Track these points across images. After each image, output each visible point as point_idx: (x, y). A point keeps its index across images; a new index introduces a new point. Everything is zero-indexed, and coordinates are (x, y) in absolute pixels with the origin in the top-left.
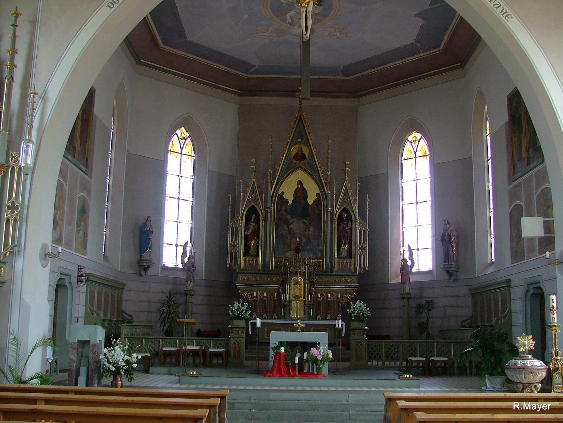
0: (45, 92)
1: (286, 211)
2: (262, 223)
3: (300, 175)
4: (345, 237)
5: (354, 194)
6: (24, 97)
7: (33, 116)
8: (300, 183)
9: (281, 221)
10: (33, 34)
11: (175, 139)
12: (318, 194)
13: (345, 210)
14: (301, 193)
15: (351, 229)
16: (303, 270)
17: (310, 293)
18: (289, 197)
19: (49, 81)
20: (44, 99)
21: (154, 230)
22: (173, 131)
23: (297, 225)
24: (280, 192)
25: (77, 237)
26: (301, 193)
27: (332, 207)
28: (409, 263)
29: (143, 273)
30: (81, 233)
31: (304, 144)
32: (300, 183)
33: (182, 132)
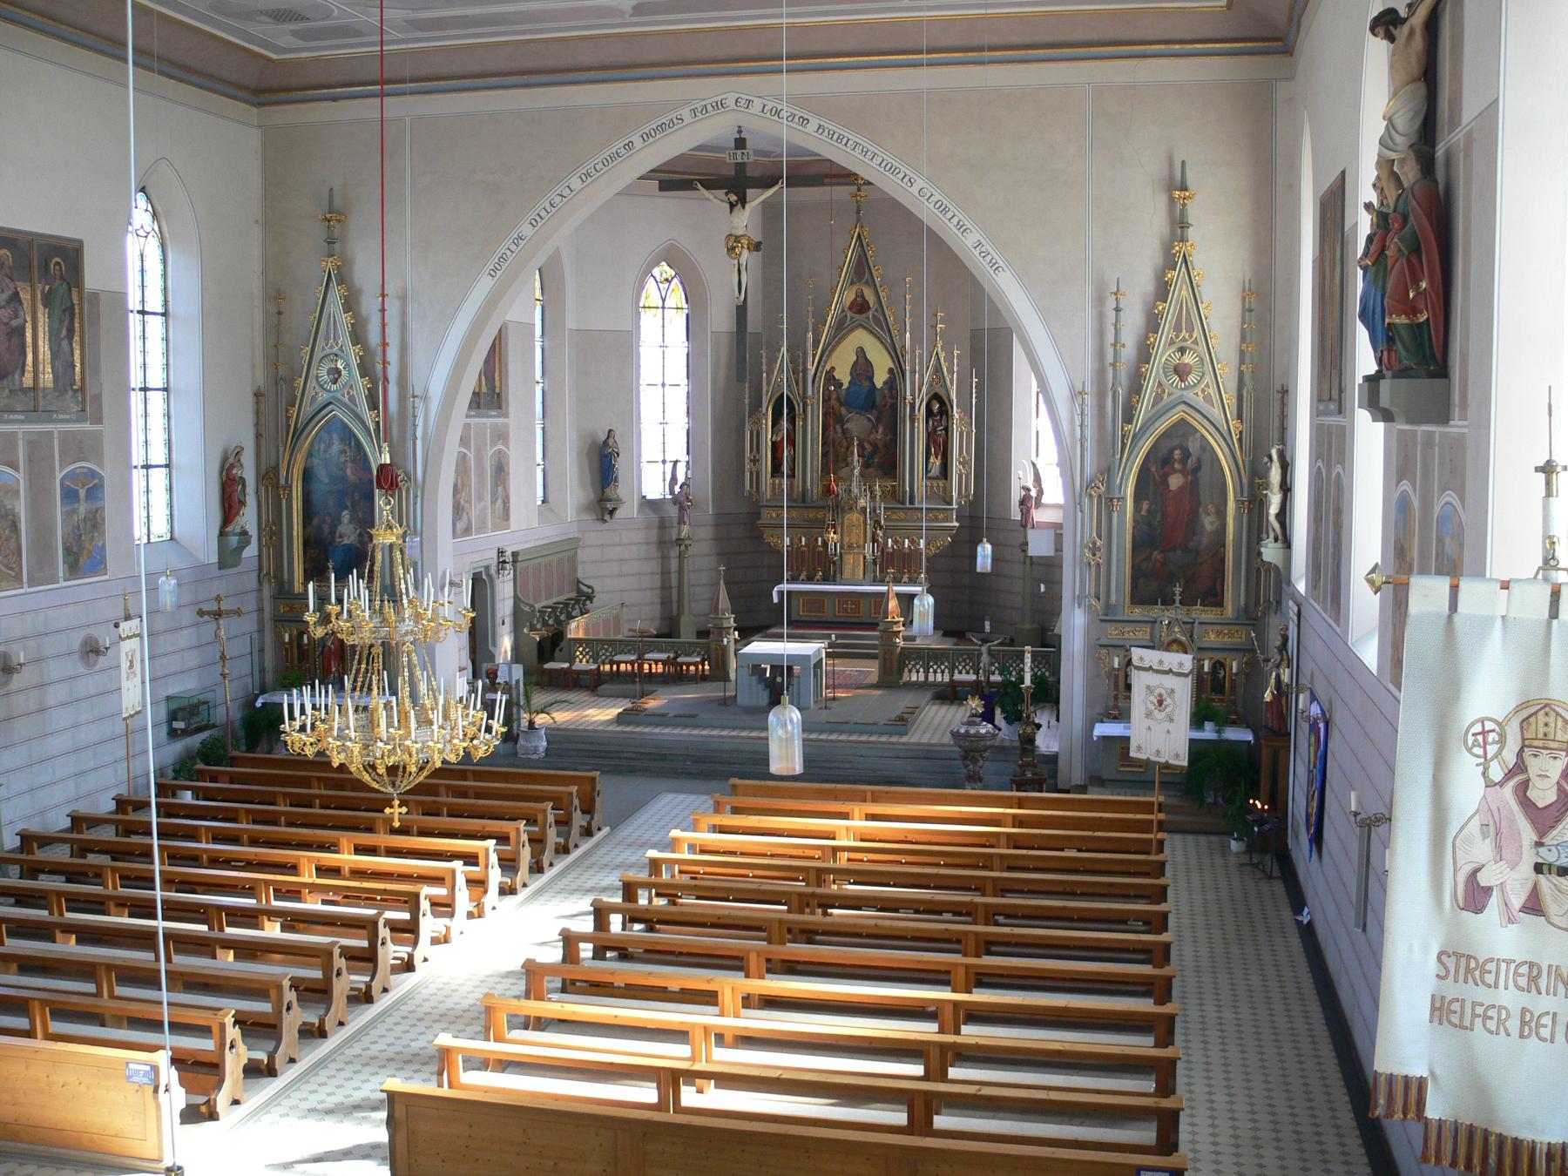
0: (426, 390)
1: (838, 399)
2: (799, 423)
3: (860, 338)
4: (939, 443)
5: (951, 372)
6: (402, 398)
7: (415, 426)
8: (861, 352)
9: (832, 418)
10: (403, 314)
11: (651, 285)
12: (891, 370)
13: (936, 397)
14: (863, 367)
15: (946, 429)
16: (862, 503)
17: (874, 540)
18: (844, 376)
19: (431, 368)
20: (426, 398)
21: (622, 448)
22: (648, 272)
23: (857, 424)
24: (828, 367)
25: (493, 511)
26: (863, 367)
27: (913, 394)
28: (1033, 493)
29: (607, 517)
30: (499, 501)
31: (867, 283)
32: (861, 352)
33: (663, 270)
